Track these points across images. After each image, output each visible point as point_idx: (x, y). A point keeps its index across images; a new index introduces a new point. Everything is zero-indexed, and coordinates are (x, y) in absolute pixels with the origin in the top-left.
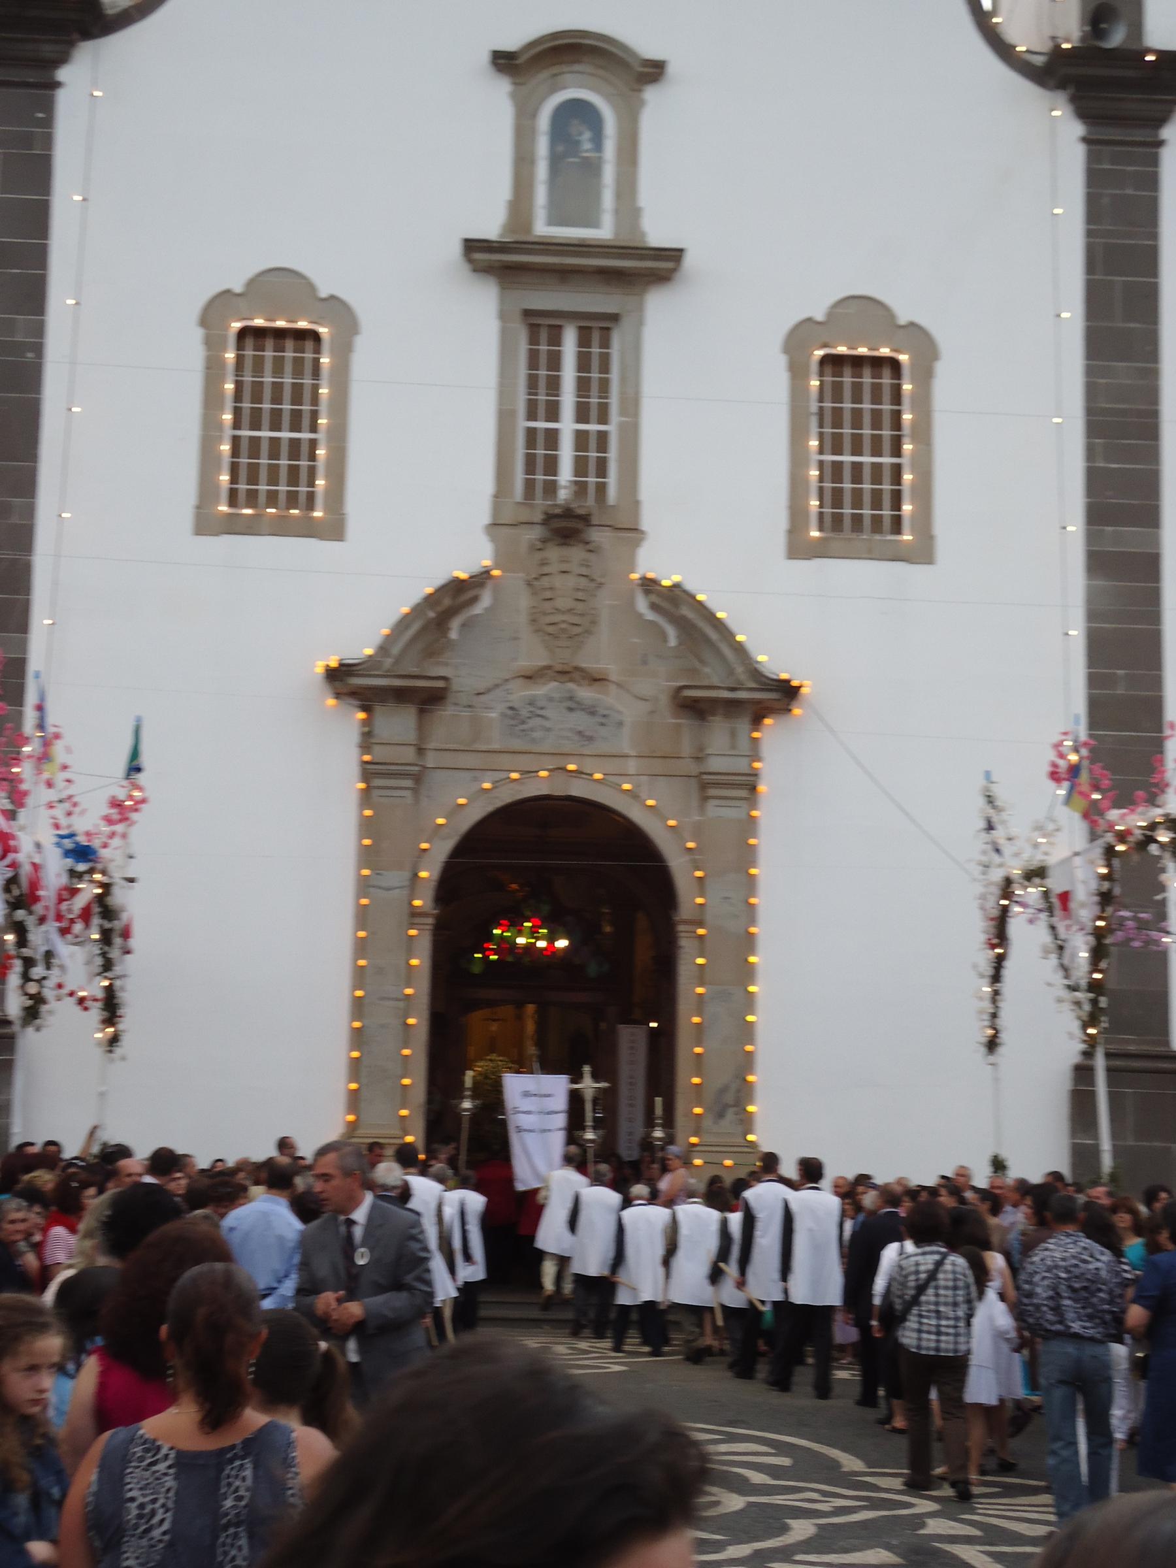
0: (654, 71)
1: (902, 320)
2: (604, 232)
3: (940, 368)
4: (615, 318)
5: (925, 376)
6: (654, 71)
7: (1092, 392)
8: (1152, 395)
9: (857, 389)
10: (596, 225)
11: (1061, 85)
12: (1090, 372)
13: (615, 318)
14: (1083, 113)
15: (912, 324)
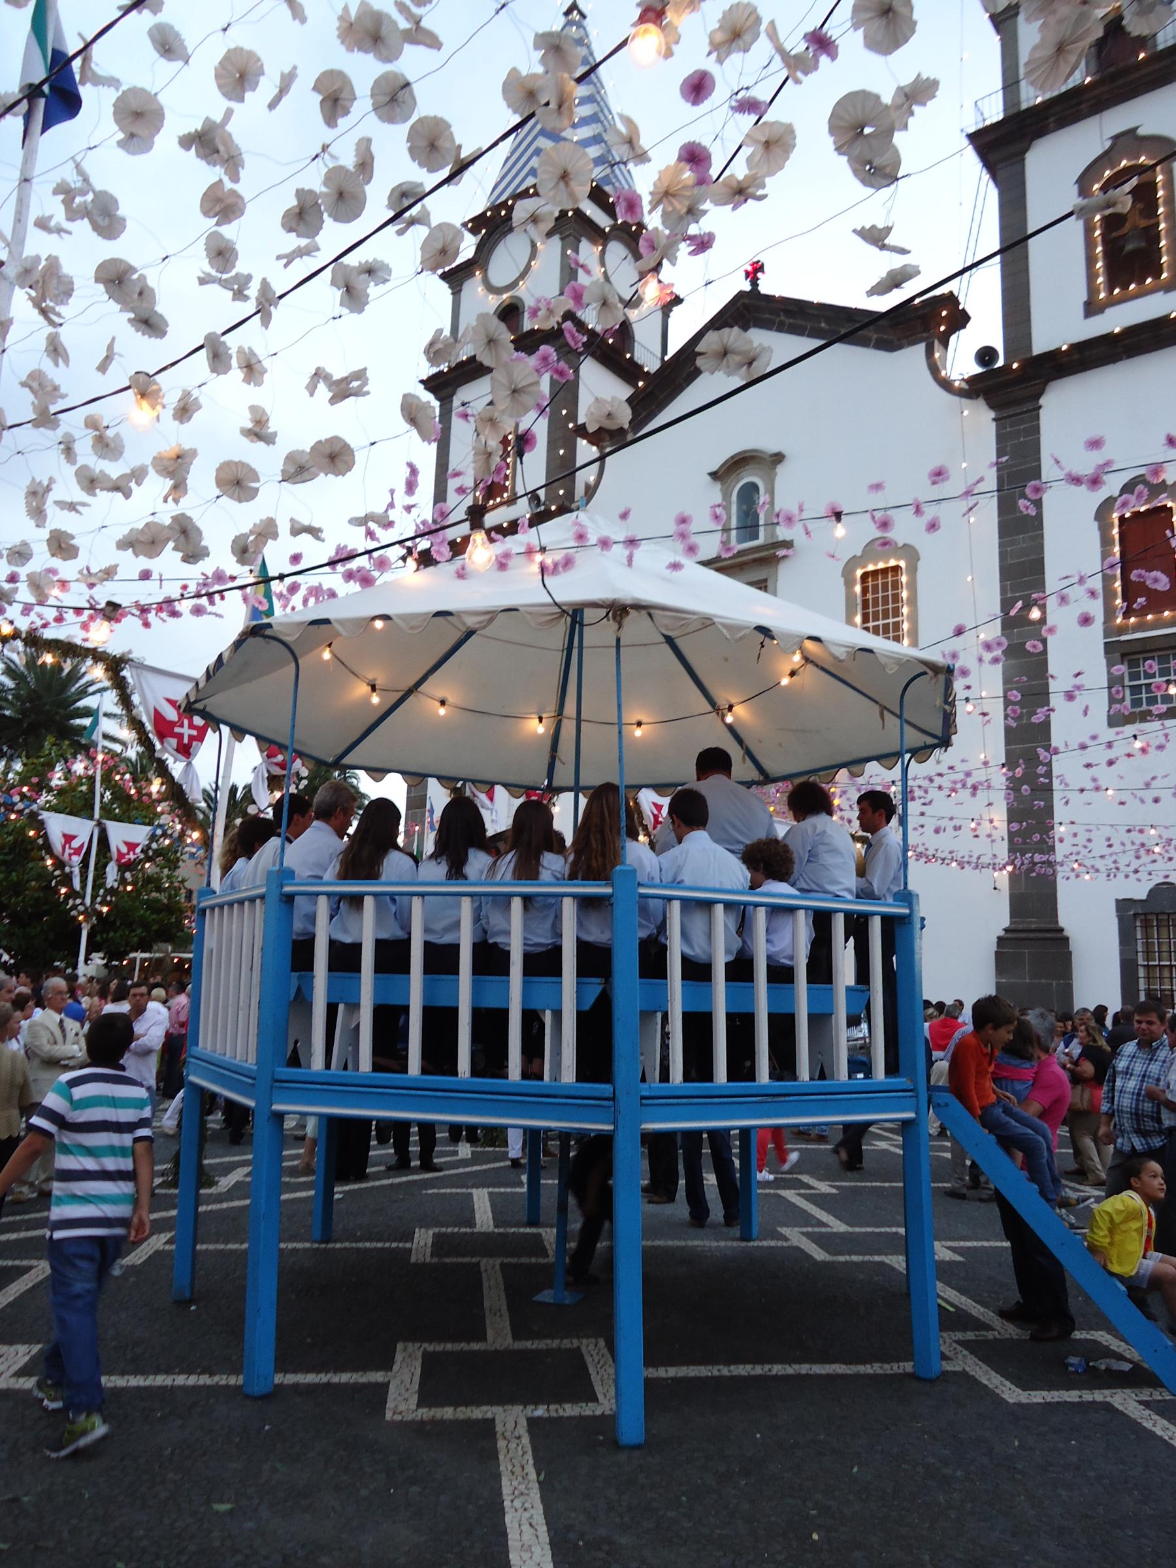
0: (778, 458)
1: (900, 544)
2: (761, 541)
3: (920, 564)
4: (765, 580)
5: (913, 570)
6: (778, 458)
7: (1003, 556)
8: (1040, 548)
9: (885, 586)
10: (757, 538)
11: (978, 397)
12: (1001, 545)
13: (765, 580)
14: (992, 406)
15: (905, 545)
